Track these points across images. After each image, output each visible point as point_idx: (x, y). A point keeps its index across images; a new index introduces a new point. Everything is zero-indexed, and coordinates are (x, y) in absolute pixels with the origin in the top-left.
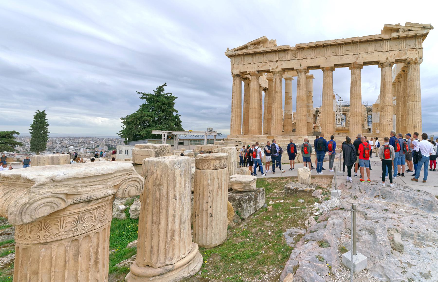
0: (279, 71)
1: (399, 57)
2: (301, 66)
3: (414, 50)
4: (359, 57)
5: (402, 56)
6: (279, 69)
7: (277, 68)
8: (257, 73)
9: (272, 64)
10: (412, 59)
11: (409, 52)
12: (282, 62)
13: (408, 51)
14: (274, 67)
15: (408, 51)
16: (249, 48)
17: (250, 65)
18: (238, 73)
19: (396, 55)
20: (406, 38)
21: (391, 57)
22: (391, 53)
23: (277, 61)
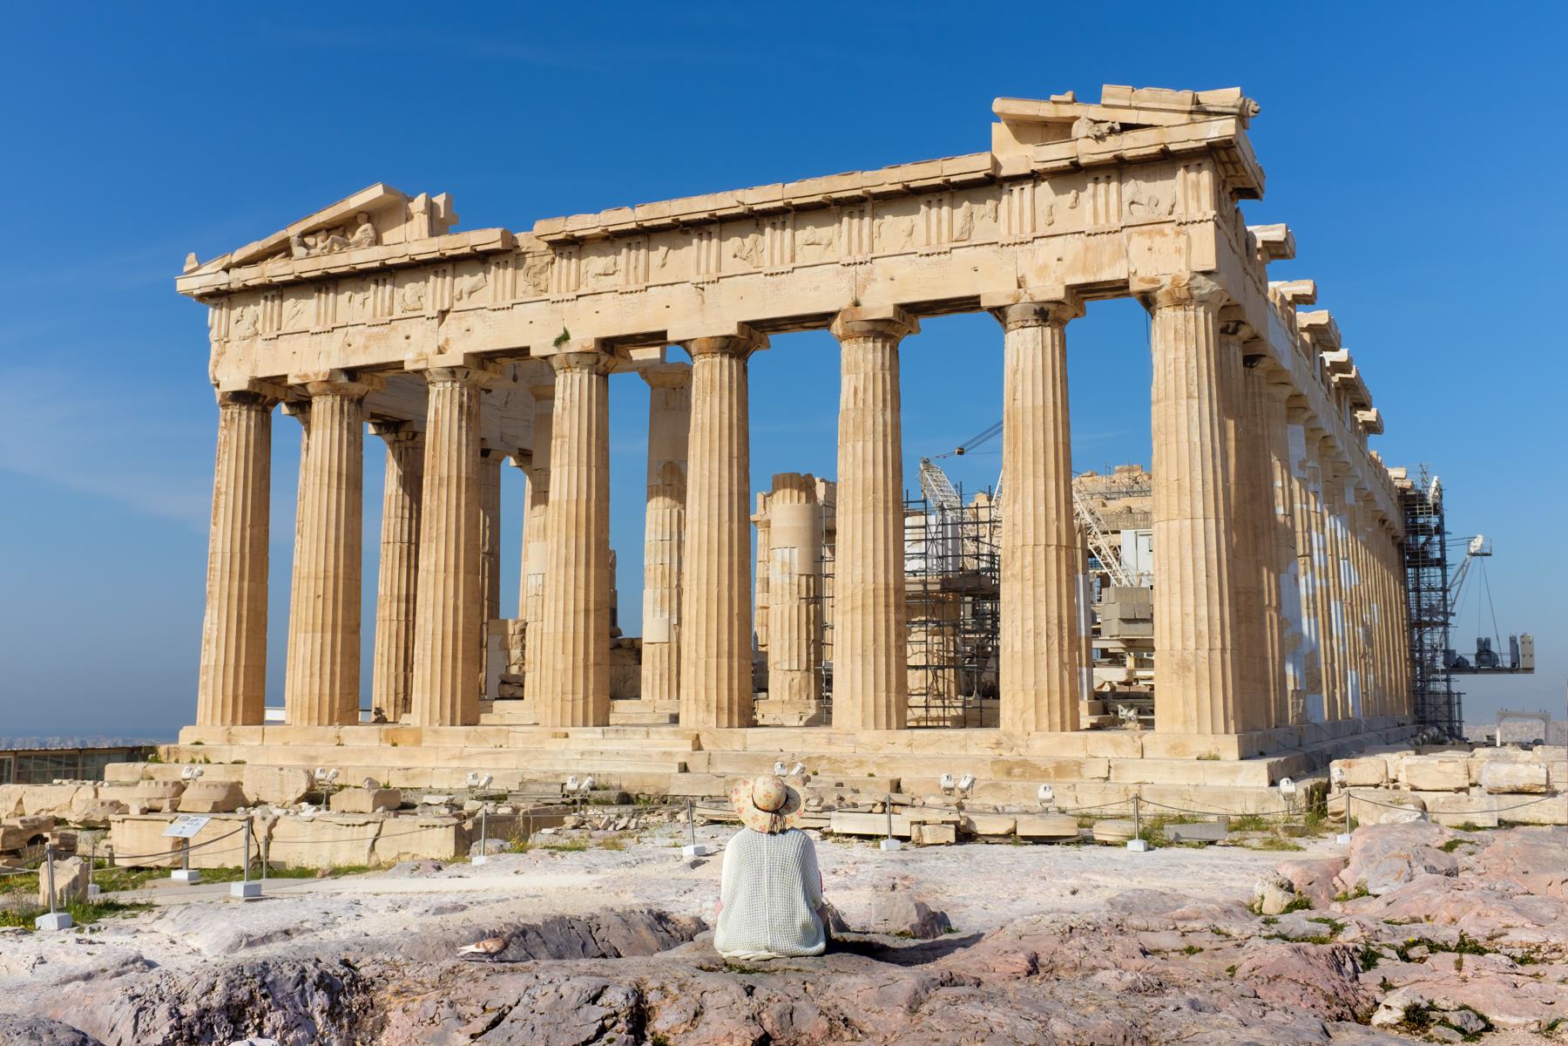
0: (453, 371)
1: (1084, 270)
2: (565, 337)
3: (1167, 228)
4: (869, 279)
5: (1100, 268)
6: (455, 358)
7: (440, 352)
8: (343, 379)
9: (418, 329)
10: (1153, 281)
11: (1138, 243)
12: (471, 320)
13: (1136, 239)
14: (431, 349)
15: (1136, 239)
16: (298, 251)
17: (306, 337)
18: (244, 386)
19: (1068, 260)
20: (1119, 168)
21: (1042, 270)
22: (1046, 251)
23: (443, 314)
